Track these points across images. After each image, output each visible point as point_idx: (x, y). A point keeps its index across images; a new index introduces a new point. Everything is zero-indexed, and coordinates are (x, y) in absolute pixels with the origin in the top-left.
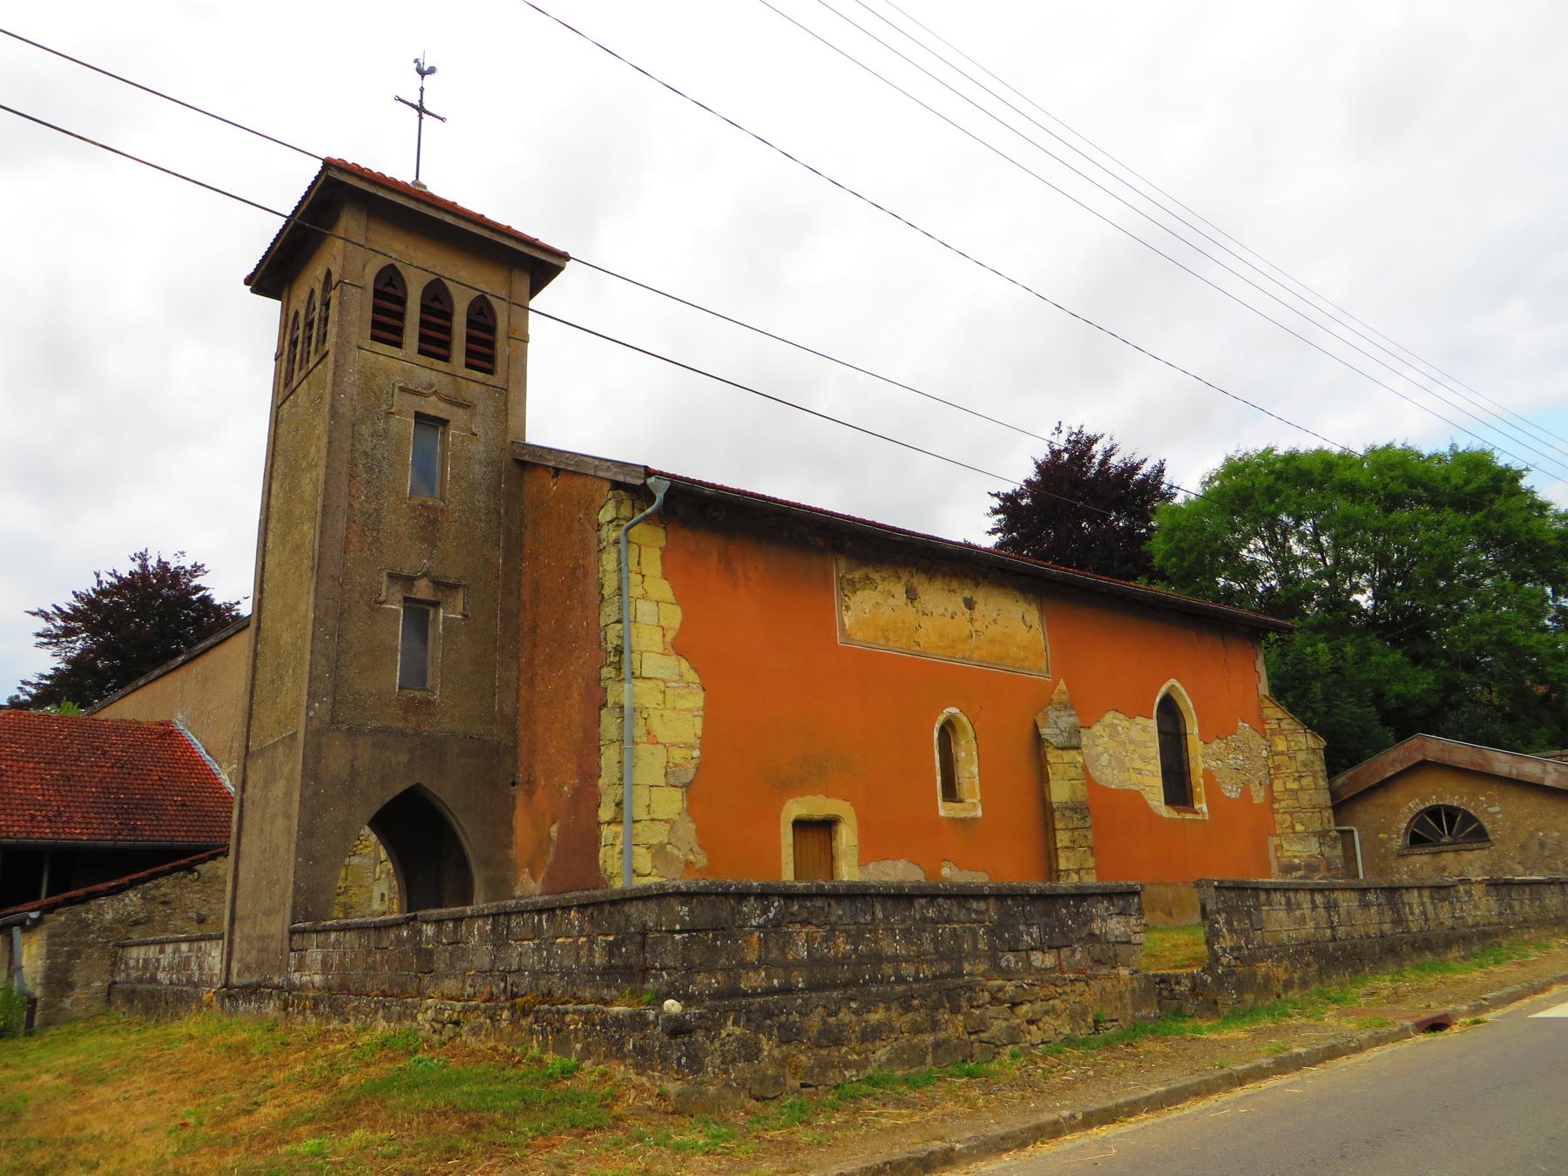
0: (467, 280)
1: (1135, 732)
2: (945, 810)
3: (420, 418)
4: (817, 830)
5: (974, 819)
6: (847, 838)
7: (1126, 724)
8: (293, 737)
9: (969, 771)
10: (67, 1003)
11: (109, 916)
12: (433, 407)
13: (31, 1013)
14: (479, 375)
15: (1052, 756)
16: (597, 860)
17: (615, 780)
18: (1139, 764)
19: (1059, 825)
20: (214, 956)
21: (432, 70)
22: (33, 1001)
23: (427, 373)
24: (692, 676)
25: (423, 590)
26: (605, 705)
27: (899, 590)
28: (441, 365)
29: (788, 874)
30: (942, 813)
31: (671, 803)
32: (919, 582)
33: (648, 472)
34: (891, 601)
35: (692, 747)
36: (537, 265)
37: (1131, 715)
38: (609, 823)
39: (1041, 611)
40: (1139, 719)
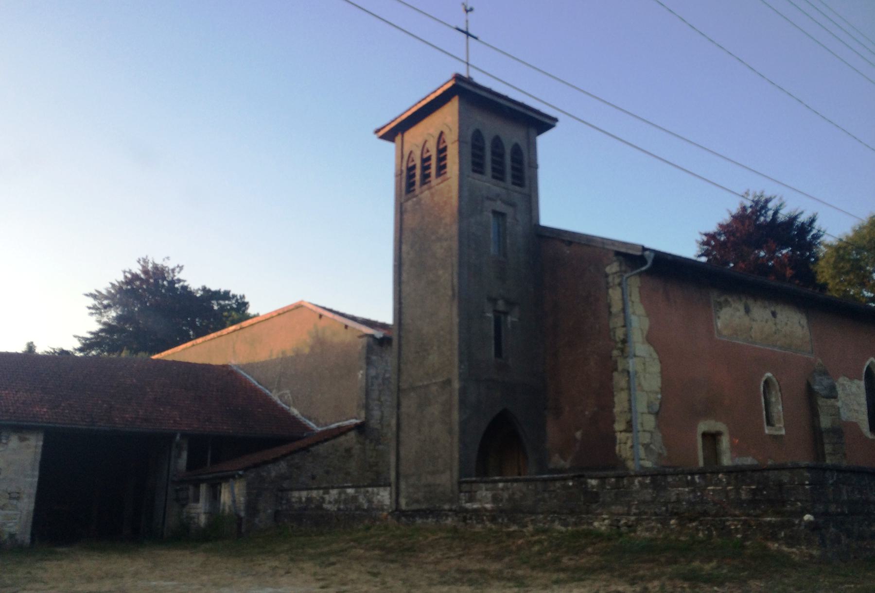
0: (511, 135)
1: (854, 389)
2: (767, 431)
3: (496, 213)
4: (711, 438)
5: (781, 436)
6: (725, 442)
7: (849, 383)
8: (448, 382)
9: (778, 409)
10: (257, 520)
11: (273, 474)
12: (499, 206)
13: (240, 526)
14: (517, 188)
15: (821, 402)
16: (614, 449)
17: (626, 409)
18: (856, 407)
19: (826, 441)
20: (384, 496)
21: (471, 10)
22: (240, 519)
23: (496, 188)
24: (655, 355)
25: (501, 305)
26: (616, 369)
27: (742, 308)
28: (502, 184)
29: (701, 463)
30: (767, 431)
31: (650, 422)
32: (750, 302)
33: (644, 249)
34: (738, 314)
35: (657, 393)
36: (542, 123)
37: (851, 378)
38: (621, 432)
39: (808, 318)
40: (856, 381)
